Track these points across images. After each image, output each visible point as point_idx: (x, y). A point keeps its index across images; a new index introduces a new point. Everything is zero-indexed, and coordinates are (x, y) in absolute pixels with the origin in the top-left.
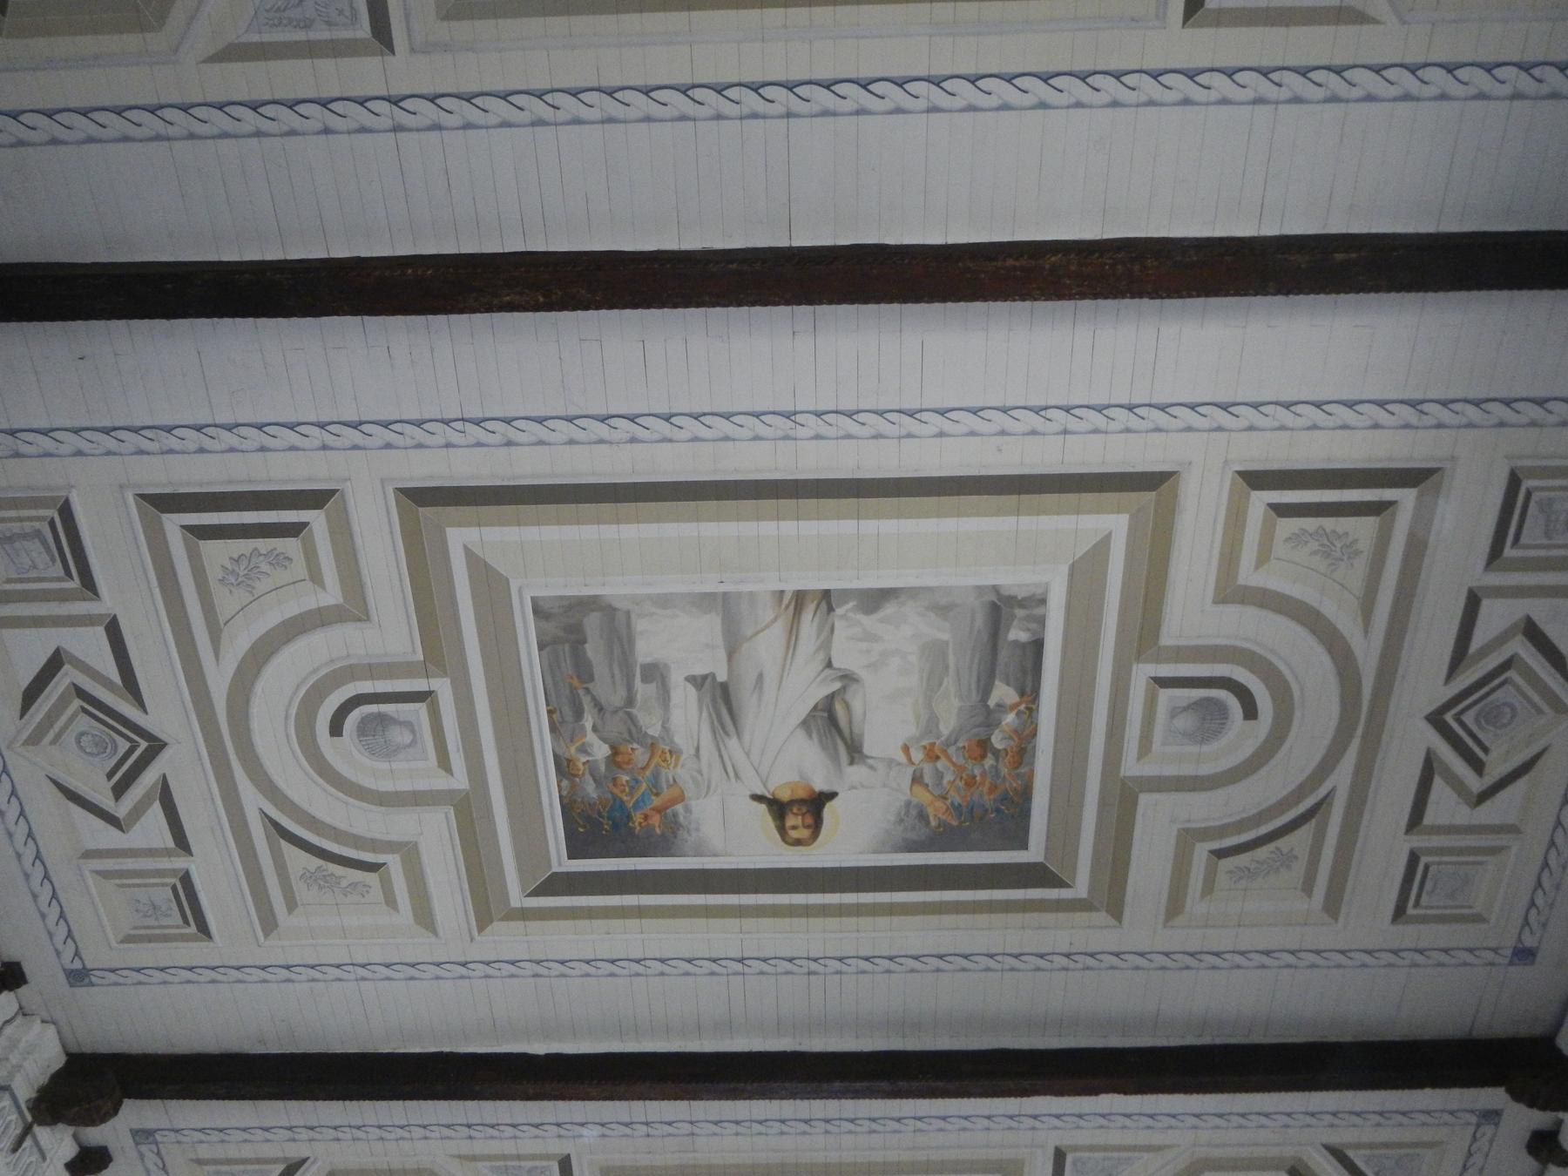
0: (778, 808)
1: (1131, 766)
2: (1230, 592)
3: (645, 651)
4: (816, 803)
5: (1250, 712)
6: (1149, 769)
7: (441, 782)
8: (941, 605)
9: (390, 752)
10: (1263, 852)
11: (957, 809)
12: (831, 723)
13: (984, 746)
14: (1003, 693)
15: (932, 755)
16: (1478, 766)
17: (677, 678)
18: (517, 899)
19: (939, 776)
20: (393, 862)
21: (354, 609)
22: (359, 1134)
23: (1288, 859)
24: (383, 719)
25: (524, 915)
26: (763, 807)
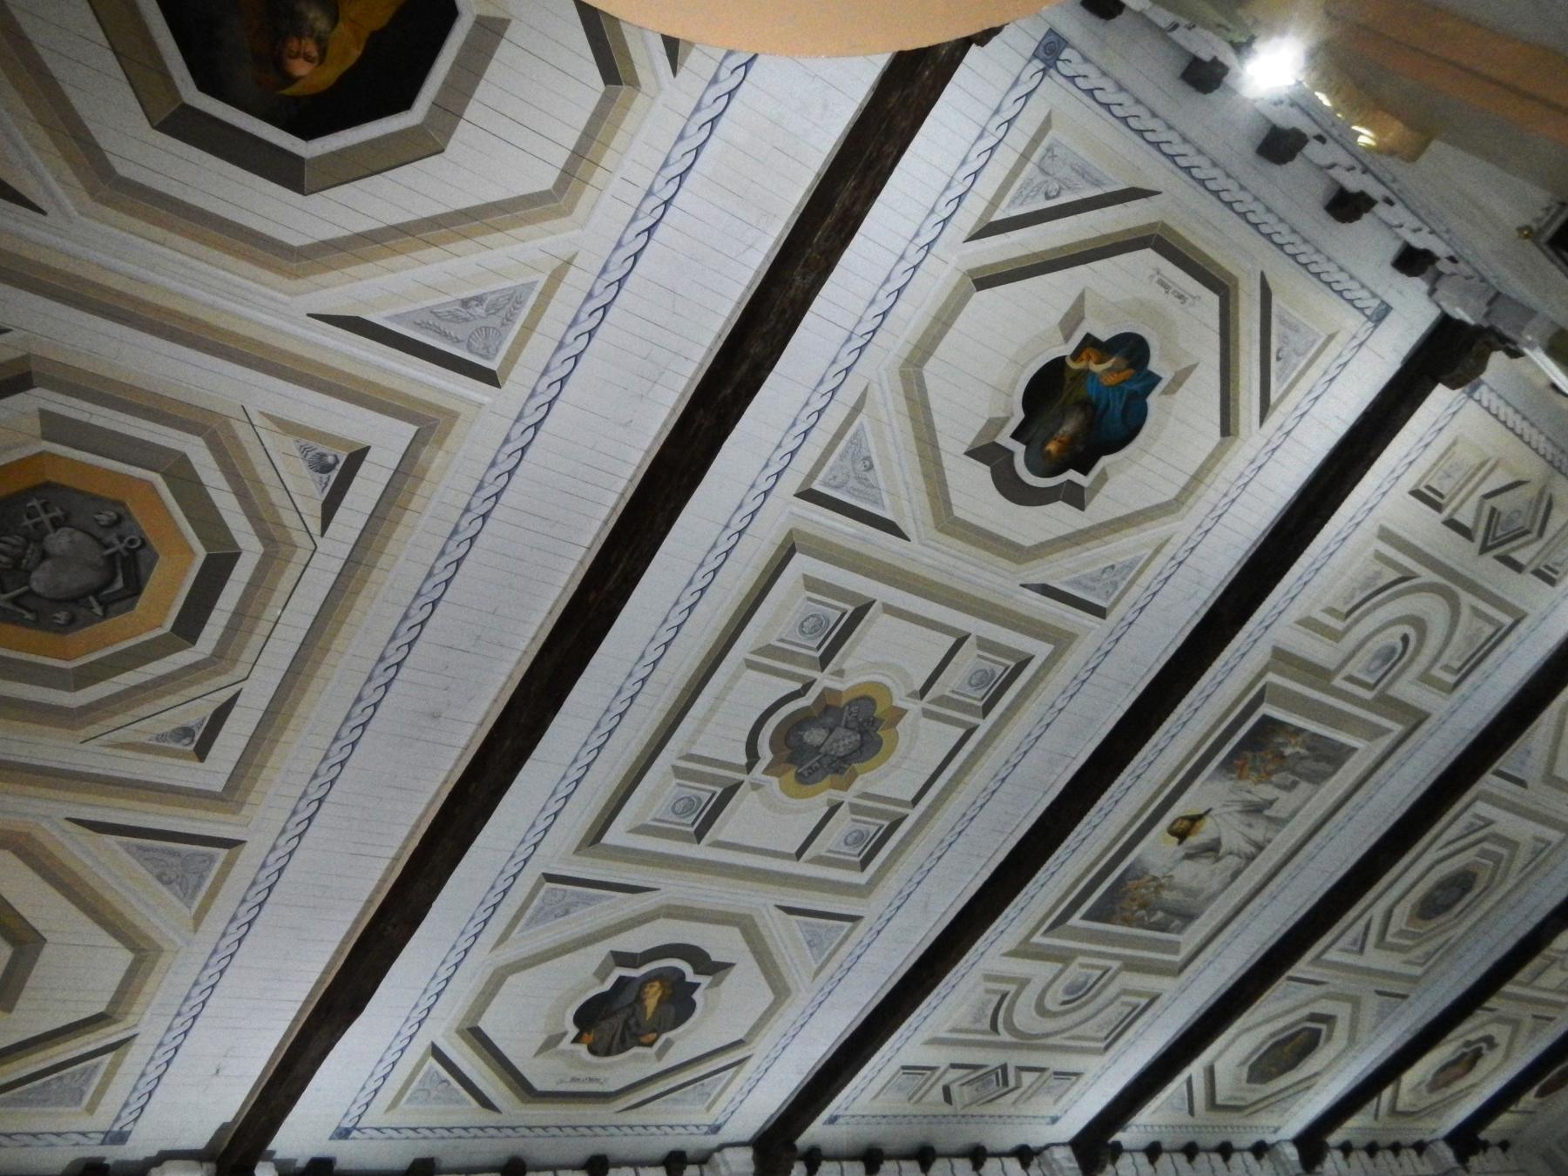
3: (1304, 786)
4: (1181, 835)
5: (1065, 1003)
7: (1344, 673)
9: (1376, 657)
10: (990, 1012)
12: (1212, 849)
13: (1143, 906)
15: (1161, 886)
17: (1283, 795)
18: (1271, 677)
20: (1338, 625)
21: (1426, 678)
22: (1241, 482)
24: (1388, 660)
25: (1261, 675)
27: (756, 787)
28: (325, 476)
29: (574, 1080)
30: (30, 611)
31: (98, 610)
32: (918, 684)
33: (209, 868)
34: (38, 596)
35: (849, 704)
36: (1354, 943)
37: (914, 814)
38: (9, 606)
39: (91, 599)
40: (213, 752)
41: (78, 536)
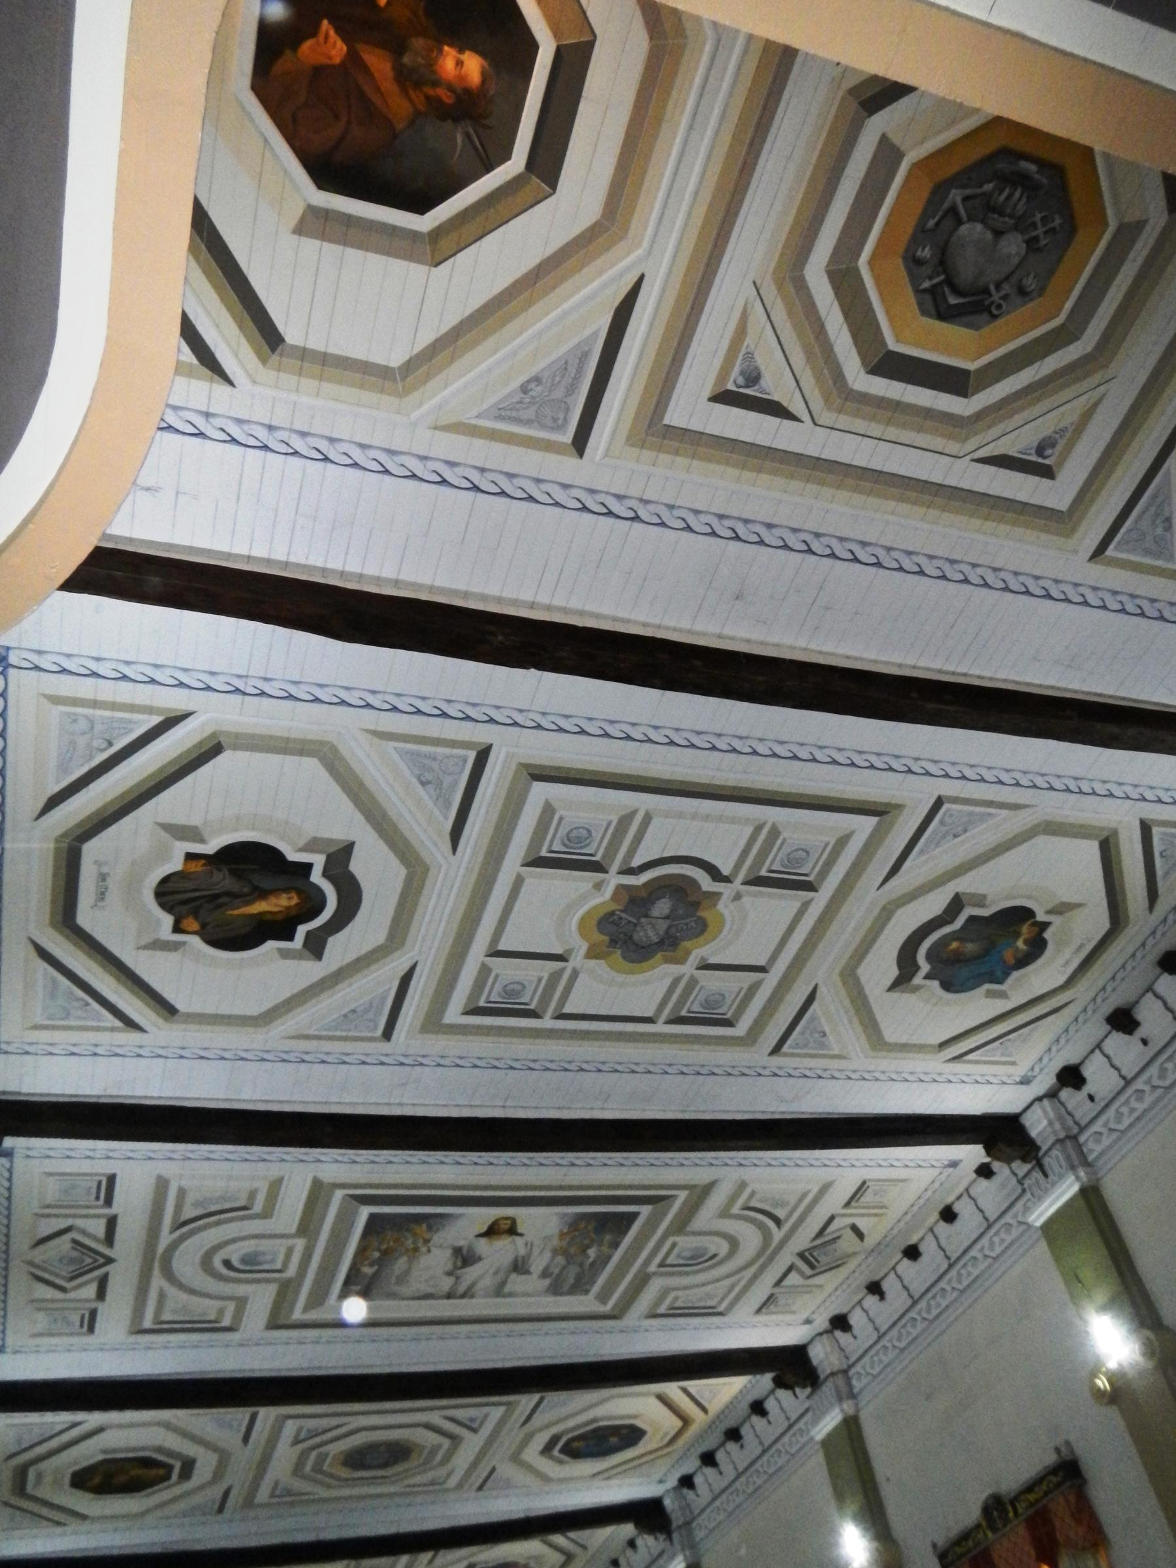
0: (512, 1231)
1: (300, 1244)
2: (241, 1303)
3: (547, 1282)
6: (290, 1242)
10: (213, 1208)
11: (408, 1230)
14: (368, 1270)
15: (416, 1250)
16: (74, 1241)
18: (682, 1195)
19: (414, 1243)
23: (197, 1204)
26: (520, 1230)
27: (598, 886)
28: (1033, 451)
29: (103, 877)
30: (937, 224)
31: (926, 284)
32: (712, 960)
33: (543, 427)
34: (956, 229)
35: (700, 918)
36: (309, 1431)
37: (547, 1023)
38: (946, 205)
39: (942, 277)
40: (717, 405)
41: (1016, 261)
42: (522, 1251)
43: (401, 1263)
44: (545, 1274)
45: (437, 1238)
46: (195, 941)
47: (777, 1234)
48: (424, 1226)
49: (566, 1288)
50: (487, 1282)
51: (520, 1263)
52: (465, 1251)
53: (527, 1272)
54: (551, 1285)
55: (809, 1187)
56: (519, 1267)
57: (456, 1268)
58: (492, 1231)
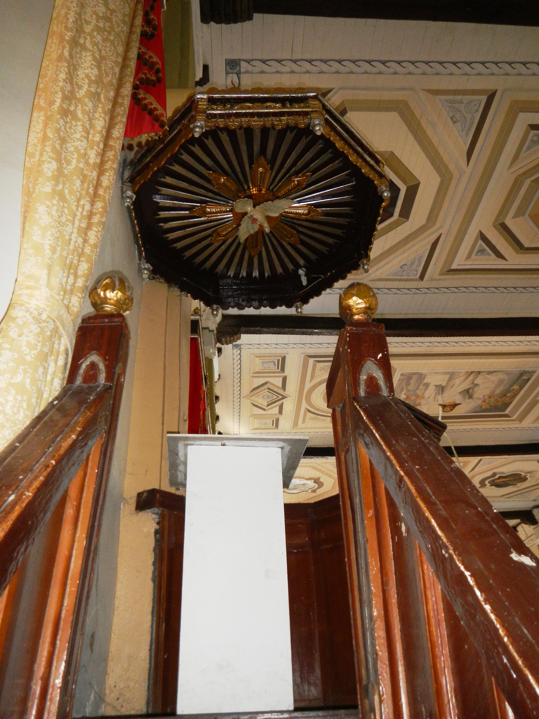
0: (444, 406)
3: (426, 381)
8: (507, 373)
13: (505, 395)
14: (516, 387)
42: (439, 397)
43: (498, 392)
44: (427, 385)
45: (480, 402)
46: (523, 474)
47: (304, 405)
48: (483, 408)
49: (415, 378)
50: (457, 381)
51: (440, 391)
52: (467, 397)
53: (436, 386)
54: (424, 379)
55: (304, 425)
56: (441, 389)
57: (473, 388)
58: (454, 405)
